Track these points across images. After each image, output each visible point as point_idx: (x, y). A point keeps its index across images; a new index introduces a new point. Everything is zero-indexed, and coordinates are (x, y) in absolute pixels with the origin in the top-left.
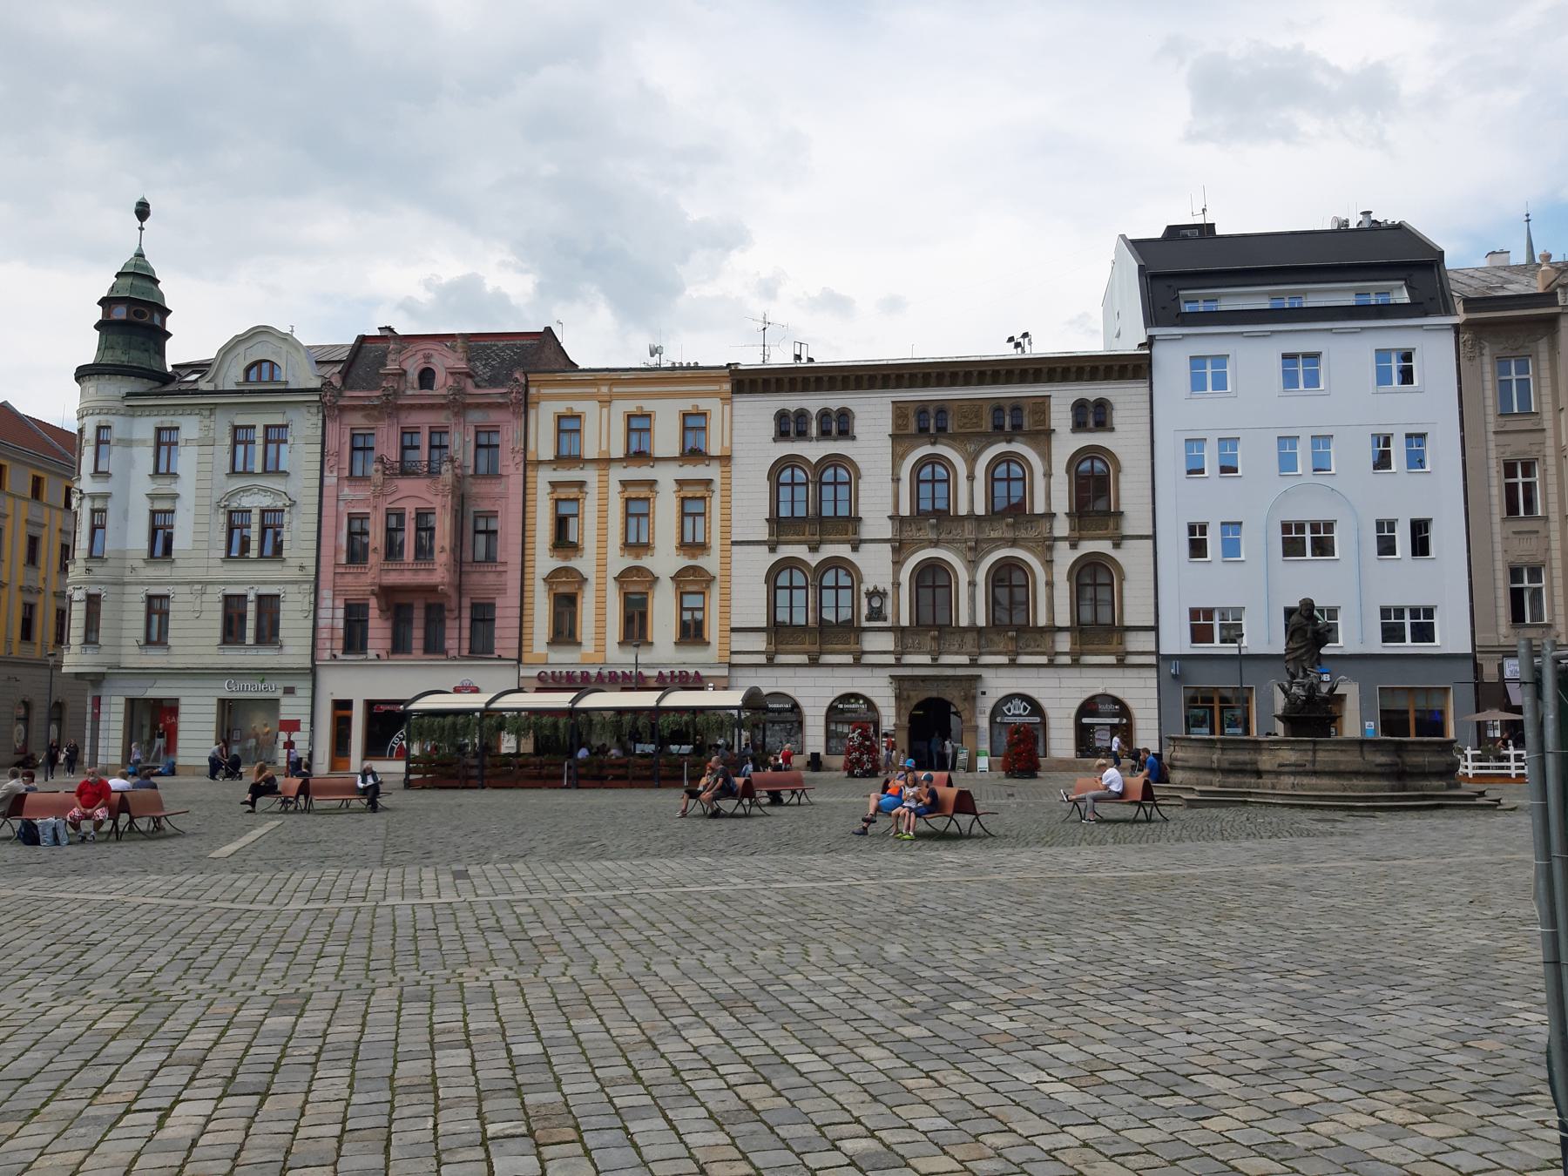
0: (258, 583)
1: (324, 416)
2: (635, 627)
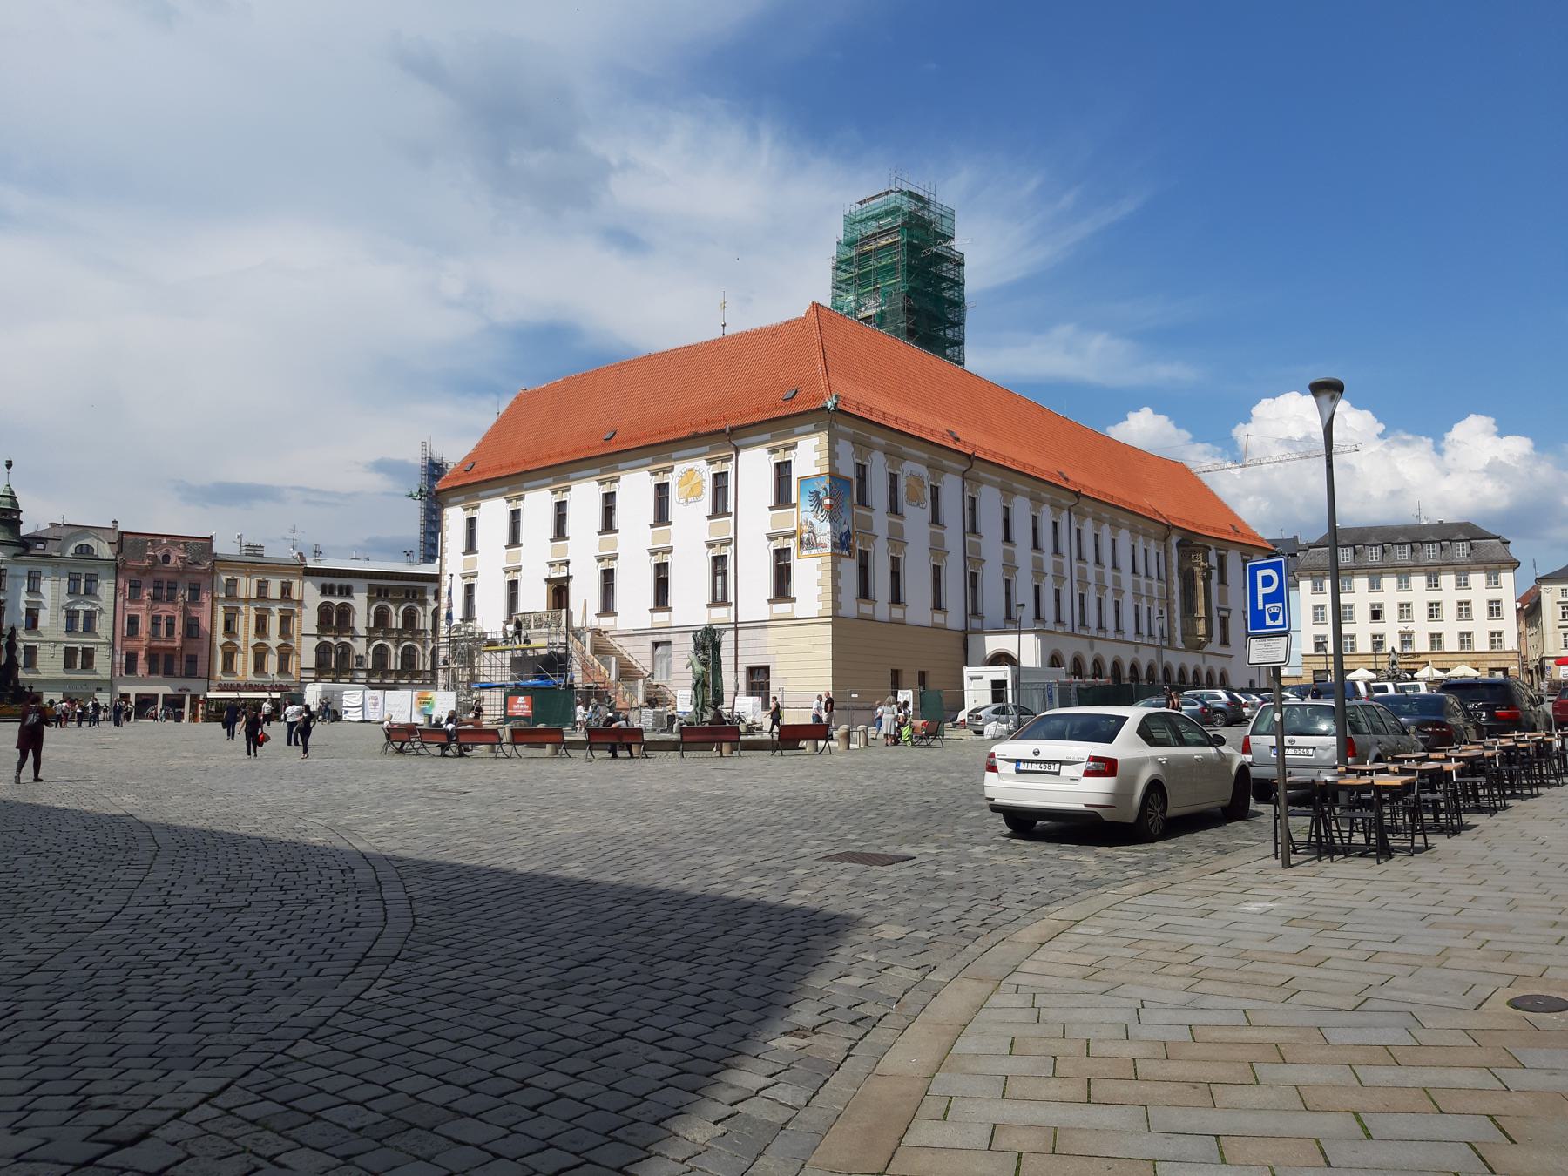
2: (259, 667)
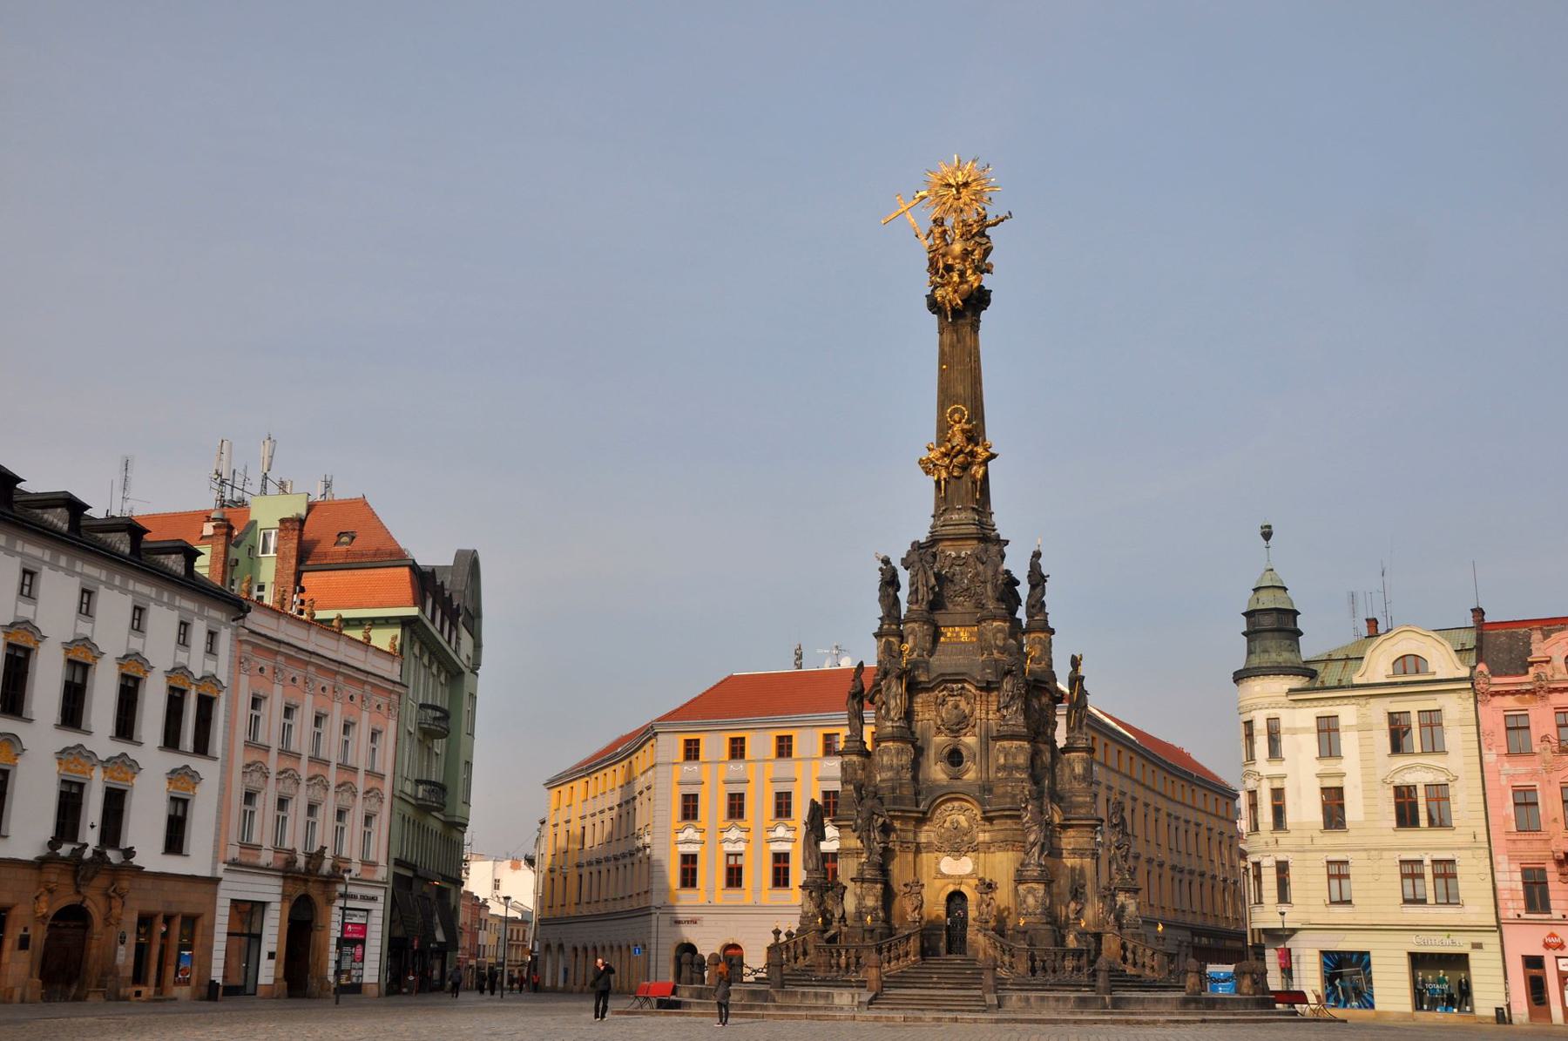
0: (1431, 849)
1: (1476, 702)
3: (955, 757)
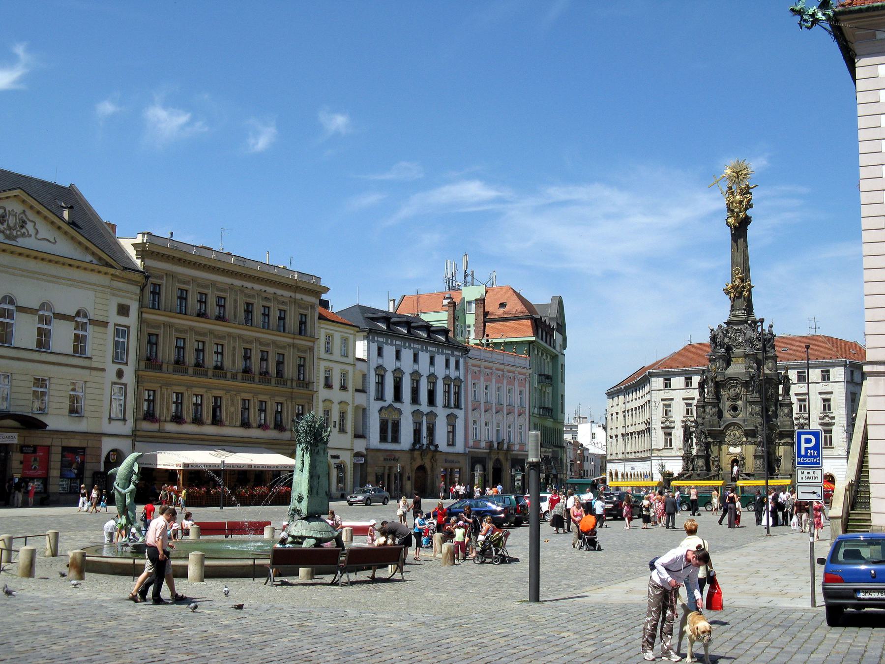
3: (735, 408)
